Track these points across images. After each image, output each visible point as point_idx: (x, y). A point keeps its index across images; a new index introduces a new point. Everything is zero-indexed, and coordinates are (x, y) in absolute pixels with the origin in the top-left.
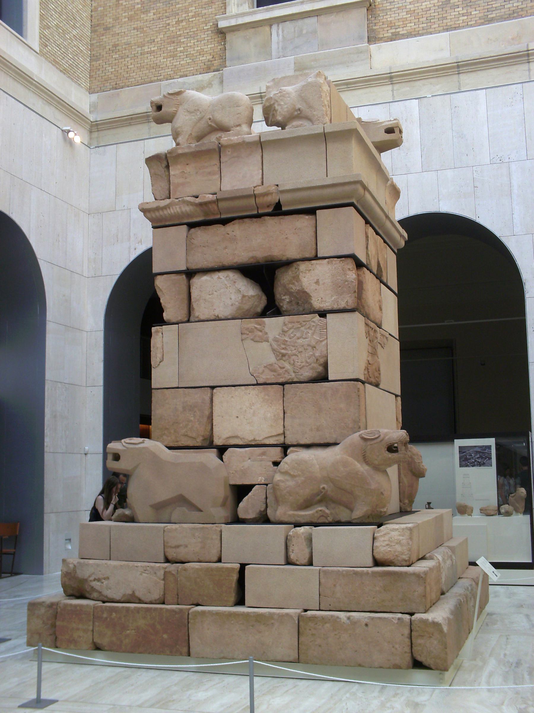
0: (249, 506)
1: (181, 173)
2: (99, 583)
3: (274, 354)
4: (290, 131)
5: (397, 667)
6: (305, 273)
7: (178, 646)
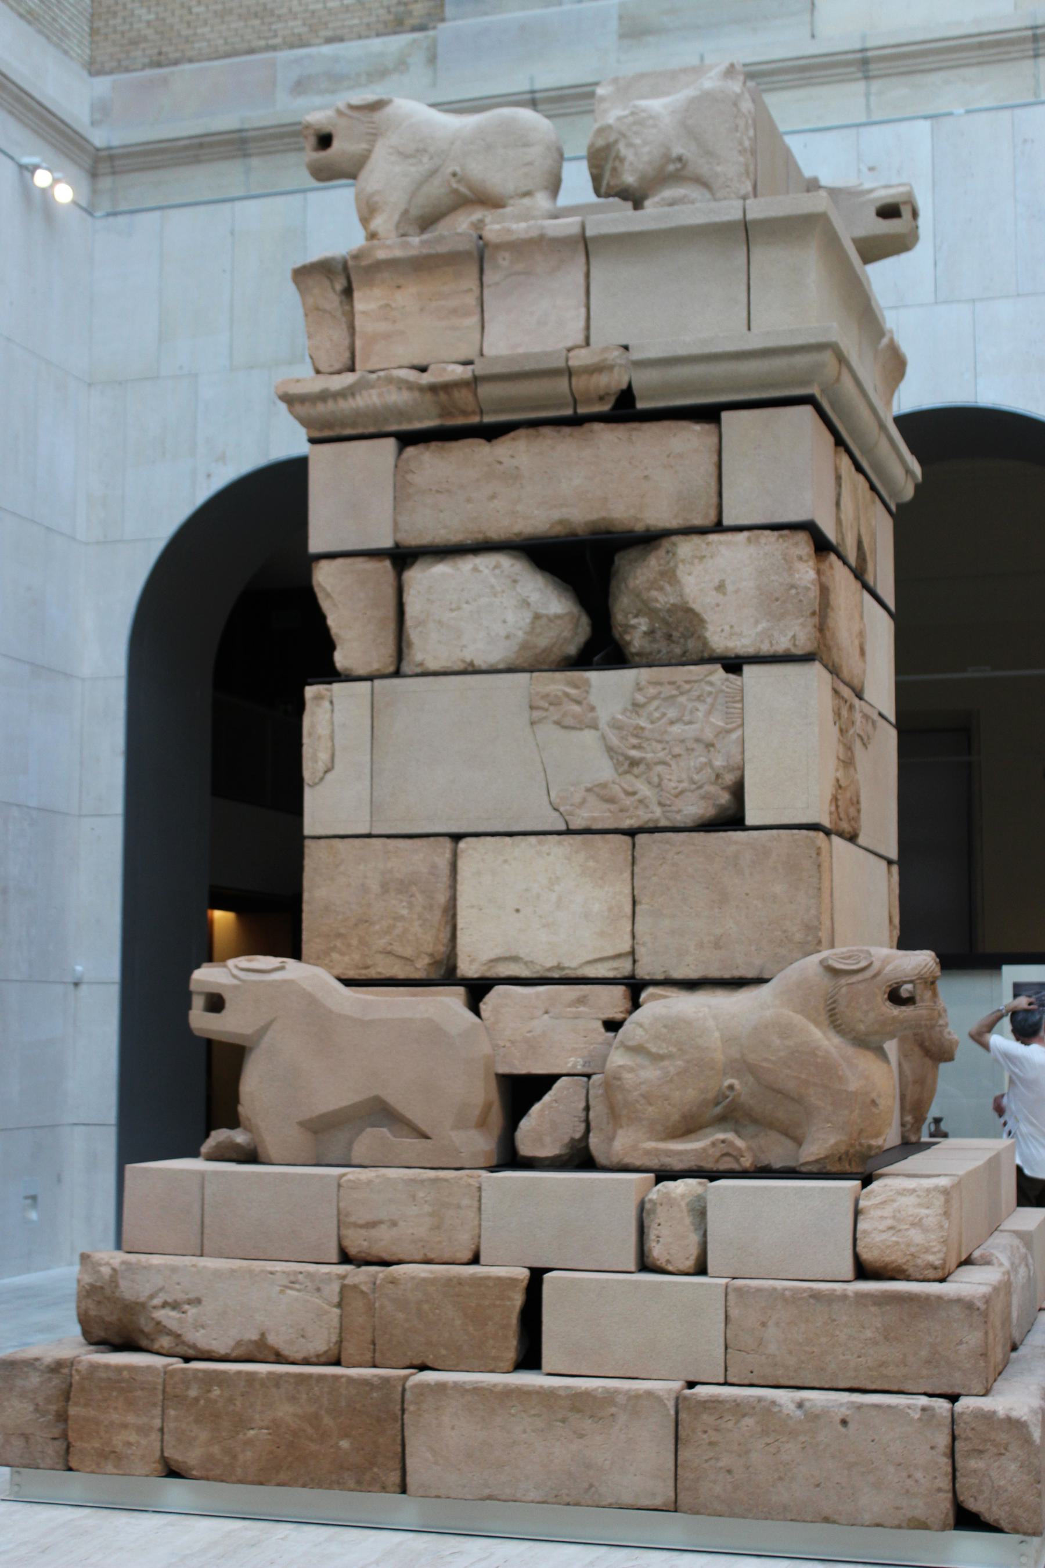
0: (542, 1127)
1: (381, 307)
2: (173, 1314)
3: (611, 758)
4: (654, 214)
5: (920, 1525)
6: (692, 563)
7: (376, 1470)
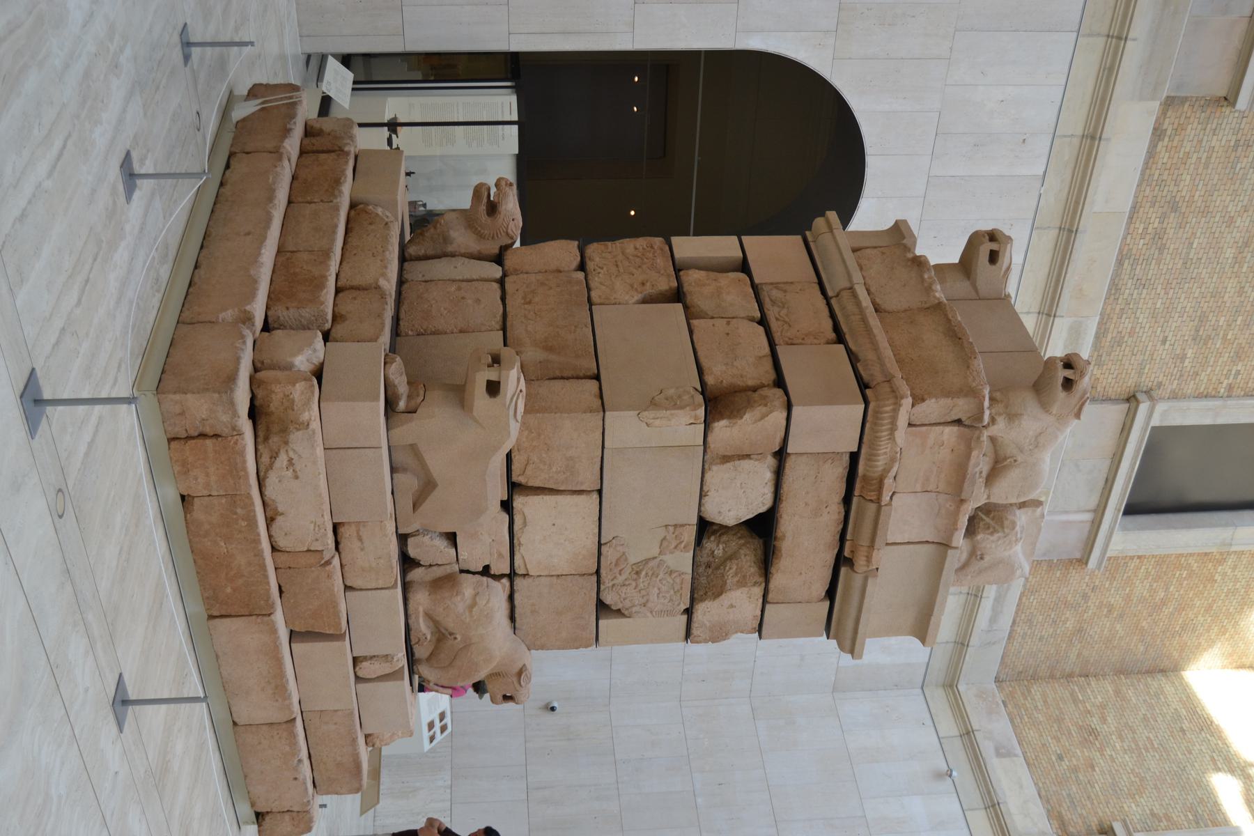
2: (285, 463)
